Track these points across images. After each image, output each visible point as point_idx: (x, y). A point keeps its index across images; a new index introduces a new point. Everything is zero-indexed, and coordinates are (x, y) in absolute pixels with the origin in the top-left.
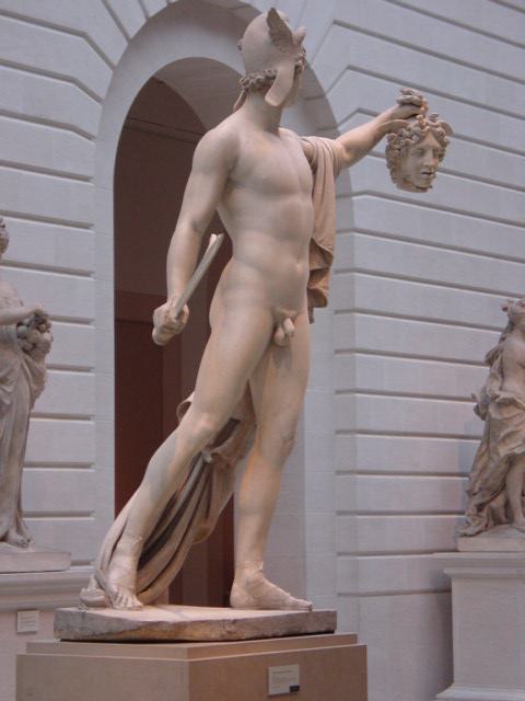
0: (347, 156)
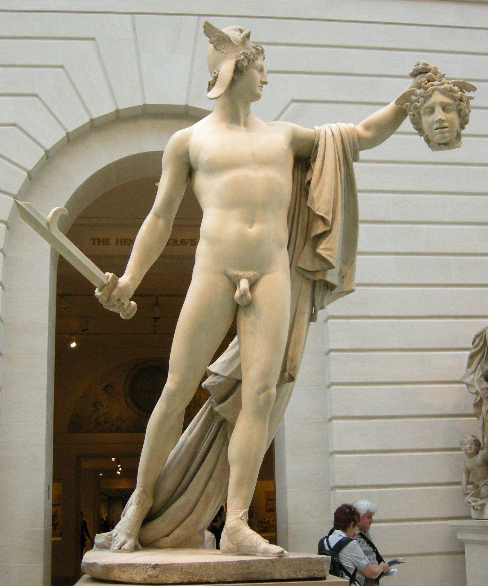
0: (368, 134)
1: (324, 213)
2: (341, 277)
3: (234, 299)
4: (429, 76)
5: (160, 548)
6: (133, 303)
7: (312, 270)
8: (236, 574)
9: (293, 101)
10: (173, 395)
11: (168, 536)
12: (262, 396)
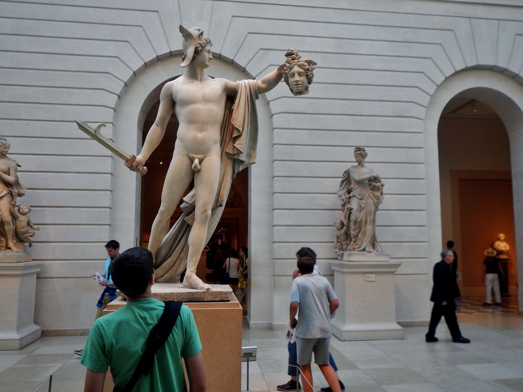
0: (263, 86)
1: (238, 126)
2: (249, 156)
3: (191, 168)
4: (293, 57)
5: (159, 282)
6: (145, 168)
7: (233, 153)
8: (186, 298)
9: (261, 49)
10: (163, 213)
11: (162, 277)
12: (204, 214)
